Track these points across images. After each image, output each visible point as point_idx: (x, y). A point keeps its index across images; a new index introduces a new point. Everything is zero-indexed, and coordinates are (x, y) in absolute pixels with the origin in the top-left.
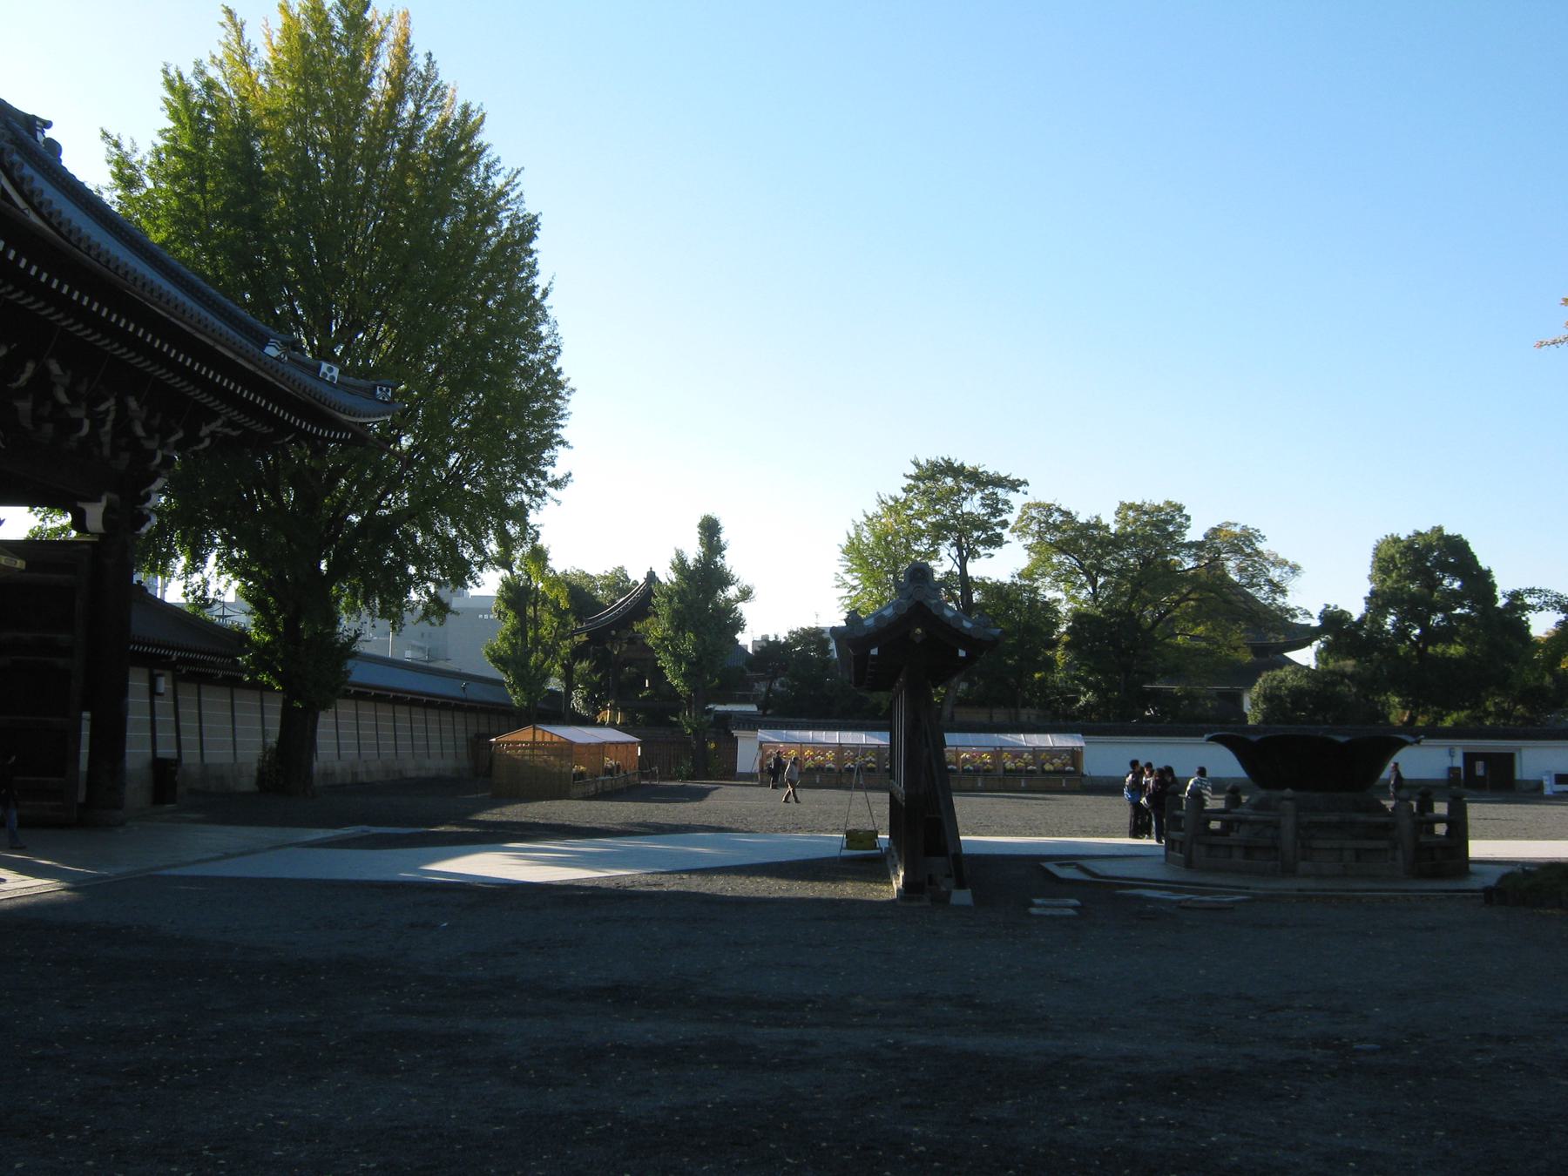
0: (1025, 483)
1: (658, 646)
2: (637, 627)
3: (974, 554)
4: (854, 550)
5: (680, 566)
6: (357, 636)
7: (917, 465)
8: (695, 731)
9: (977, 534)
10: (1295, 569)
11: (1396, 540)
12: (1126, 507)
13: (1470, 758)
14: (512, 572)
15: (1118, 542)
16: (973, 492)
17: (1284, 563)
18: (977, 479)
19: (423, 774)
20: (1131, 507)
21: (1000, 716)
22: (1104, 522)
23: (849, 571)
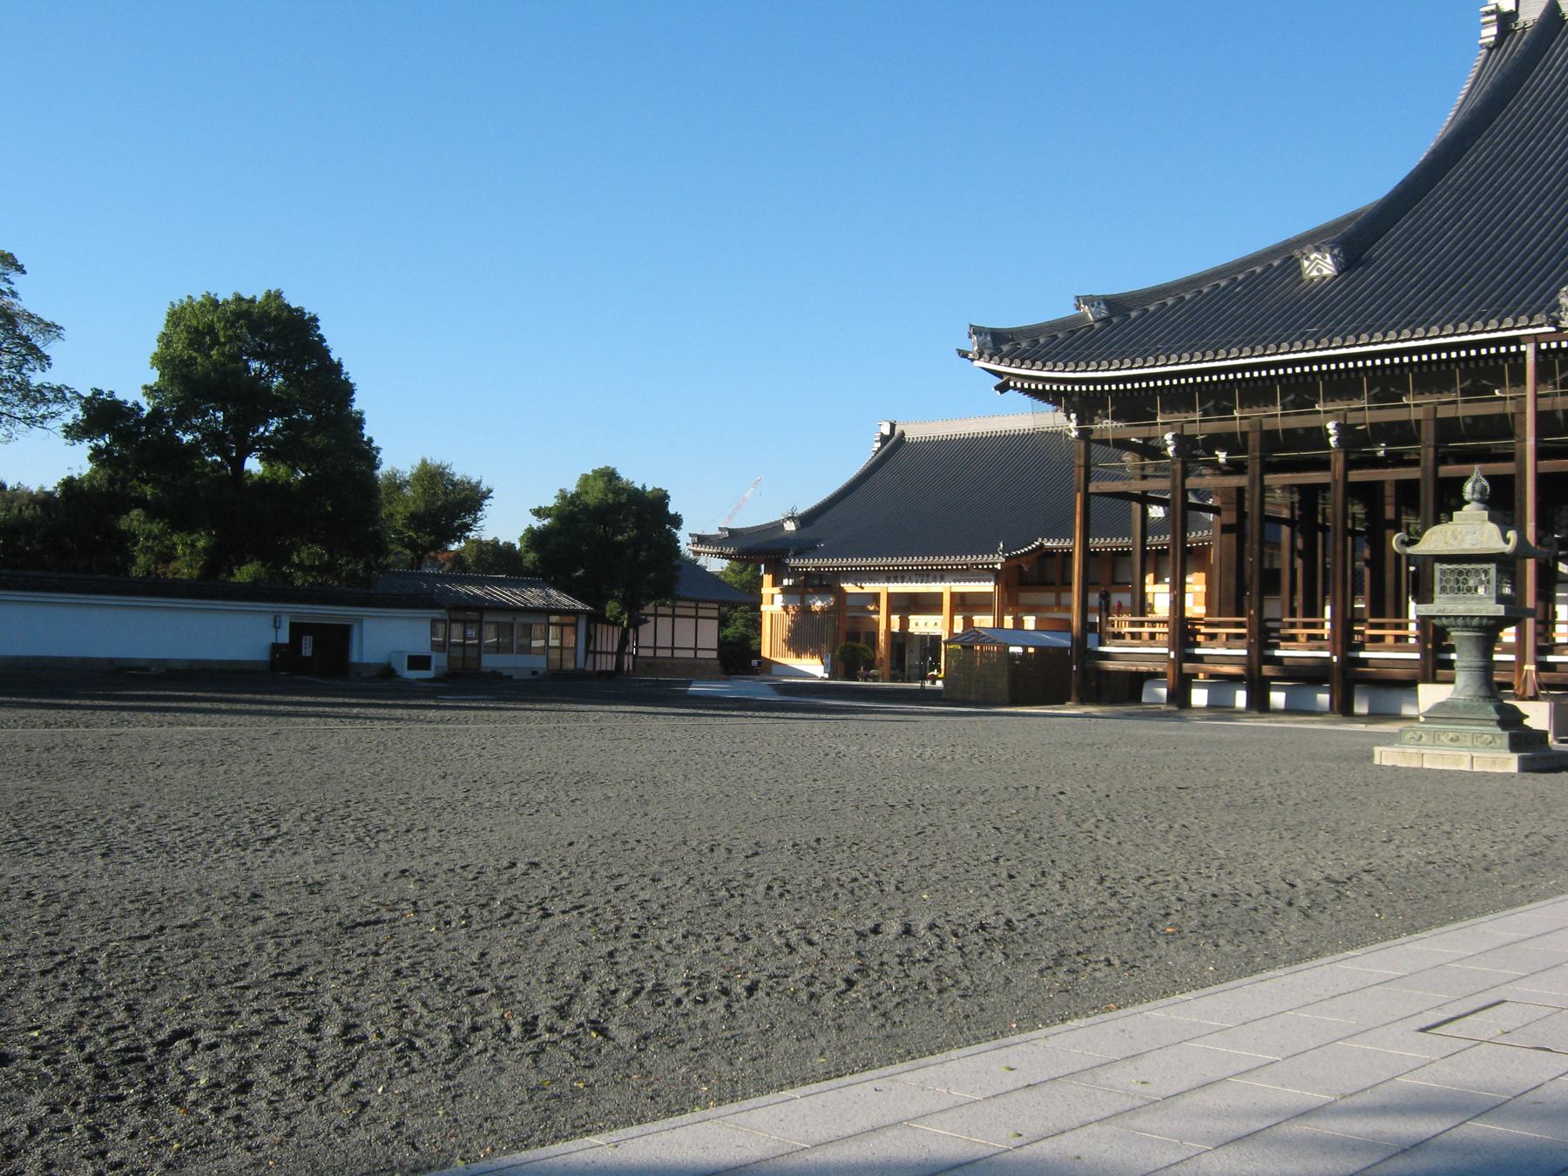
10: (50, 328)
11: (215, 304)
13: (297, 630)
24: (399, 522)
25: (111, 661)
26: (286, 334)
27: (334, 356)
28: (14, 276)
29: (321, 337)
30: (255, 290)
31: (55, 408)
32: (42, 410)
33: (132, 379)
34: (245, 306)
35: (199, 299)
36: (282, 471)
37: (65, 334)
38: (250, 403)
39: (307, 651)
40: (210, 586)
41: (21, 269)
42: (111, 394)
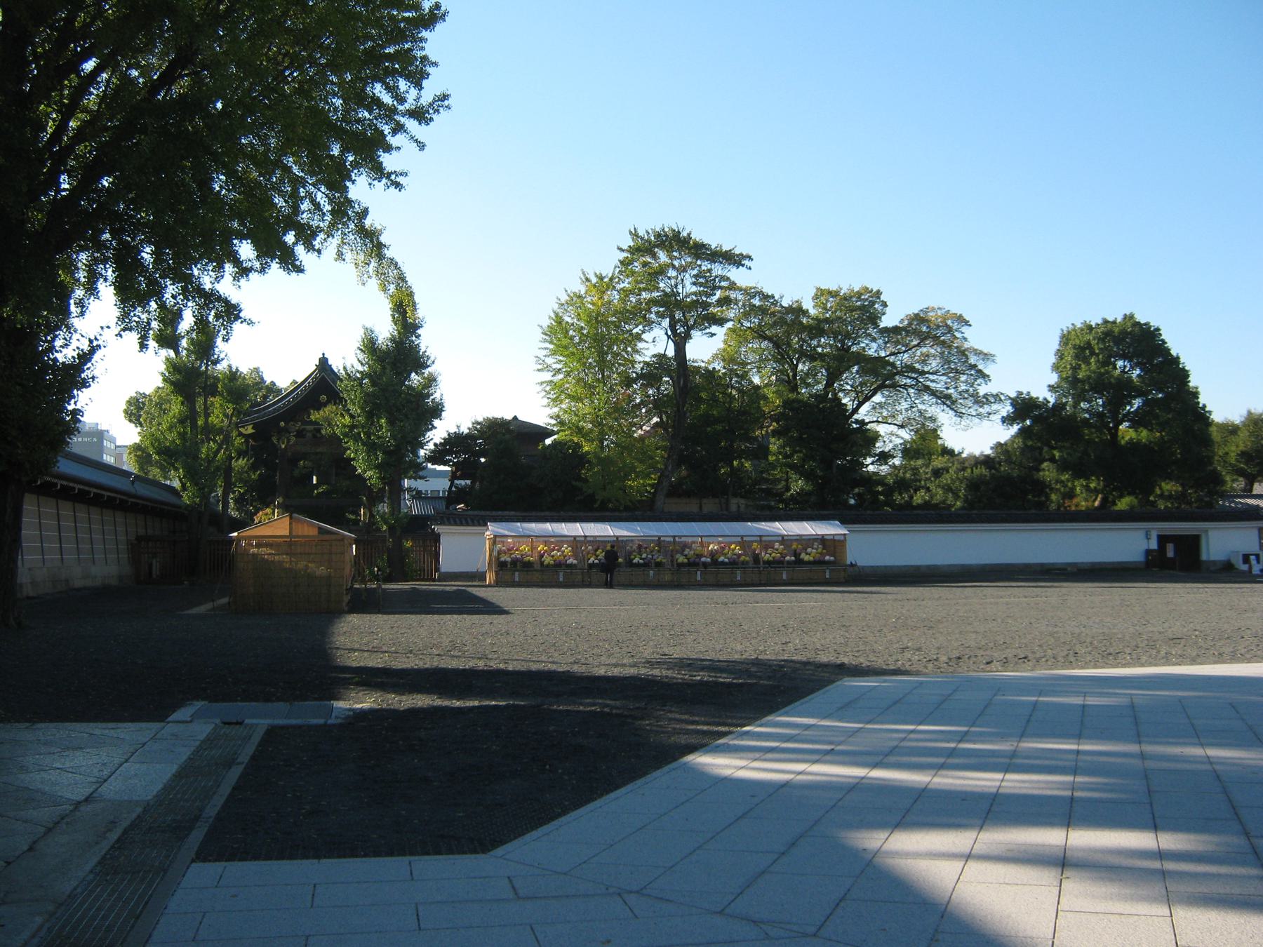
0: (750, 258)
1: (346, 435)
2: (315, 416)
3: (688, 336)
4: (557, 331)
5: (370, 345)
6: (93, 350)
7: (635, 235)
8: (391, 528)
9: (686, 316)
10: (987, 357)
11: (1090, 328)
12: (820, 294)
13: (1163, 540)
14: (177, 352)
15: (818, 328)
16: (682, 269)
17: (981, 353)
18: (699, 250)
19: (89, 583)
20: (830, 293)
21: (710, 505)
22: (804, 308)
23: (554, 353)
24: (1232, 458)
25: (1042, 565)
26: (1140, 342)
27: (1174, 352)
28: (964, 329)
29: (1163, 341)
30: (1116, 315)
31: (995, 407)
32: (986, 409)
33: (1039, 381)
34: (1109, 326)
35: (1079, 325)
36: (1144, 433)
37: (997, 359)
38: (1119, 391)
39: (1170, 553)
40: (1103, 515)
41: (967, 323)
42: (1028, 393)
